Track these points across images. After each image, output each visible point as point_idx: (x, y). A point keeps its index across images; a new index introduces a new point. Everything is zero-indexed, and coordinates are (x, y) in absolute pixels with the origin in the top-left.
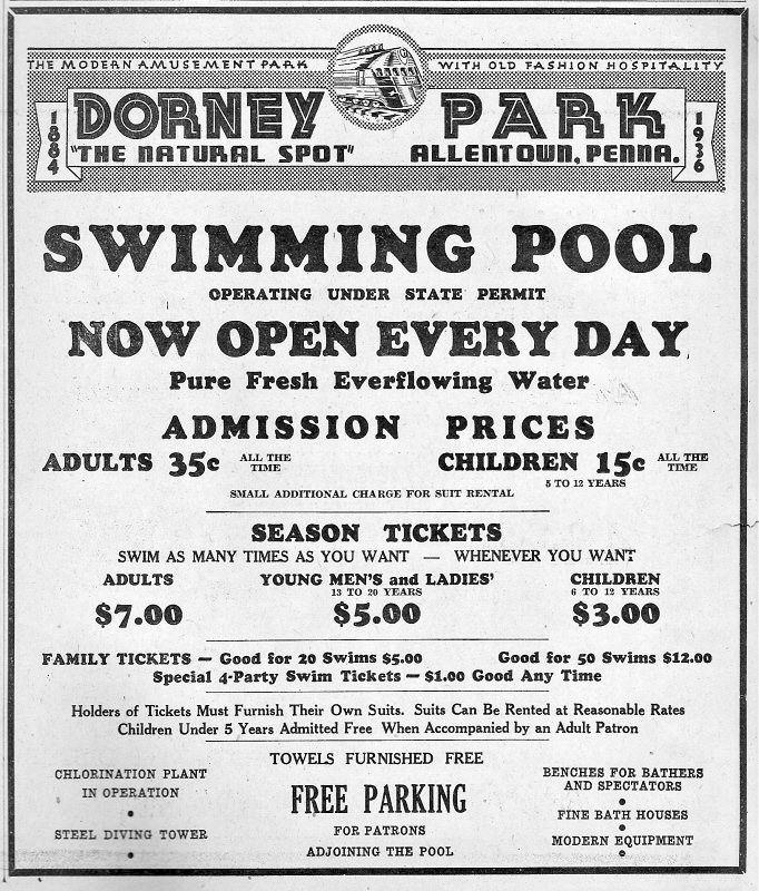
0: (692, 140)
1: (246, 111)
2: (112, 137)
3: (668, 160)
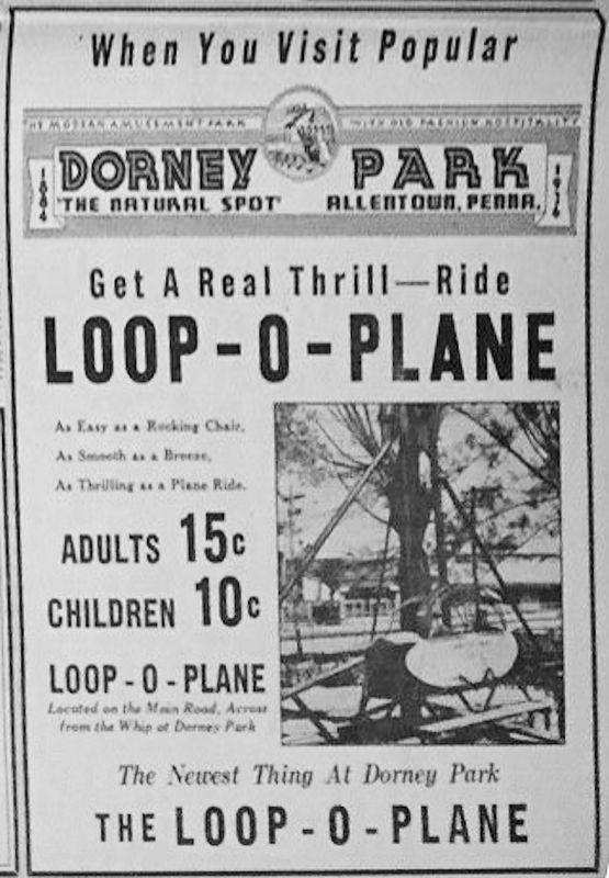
0: (552, 188)
1: (195, 165)
2: (89, 189)
3: (532, 206)
